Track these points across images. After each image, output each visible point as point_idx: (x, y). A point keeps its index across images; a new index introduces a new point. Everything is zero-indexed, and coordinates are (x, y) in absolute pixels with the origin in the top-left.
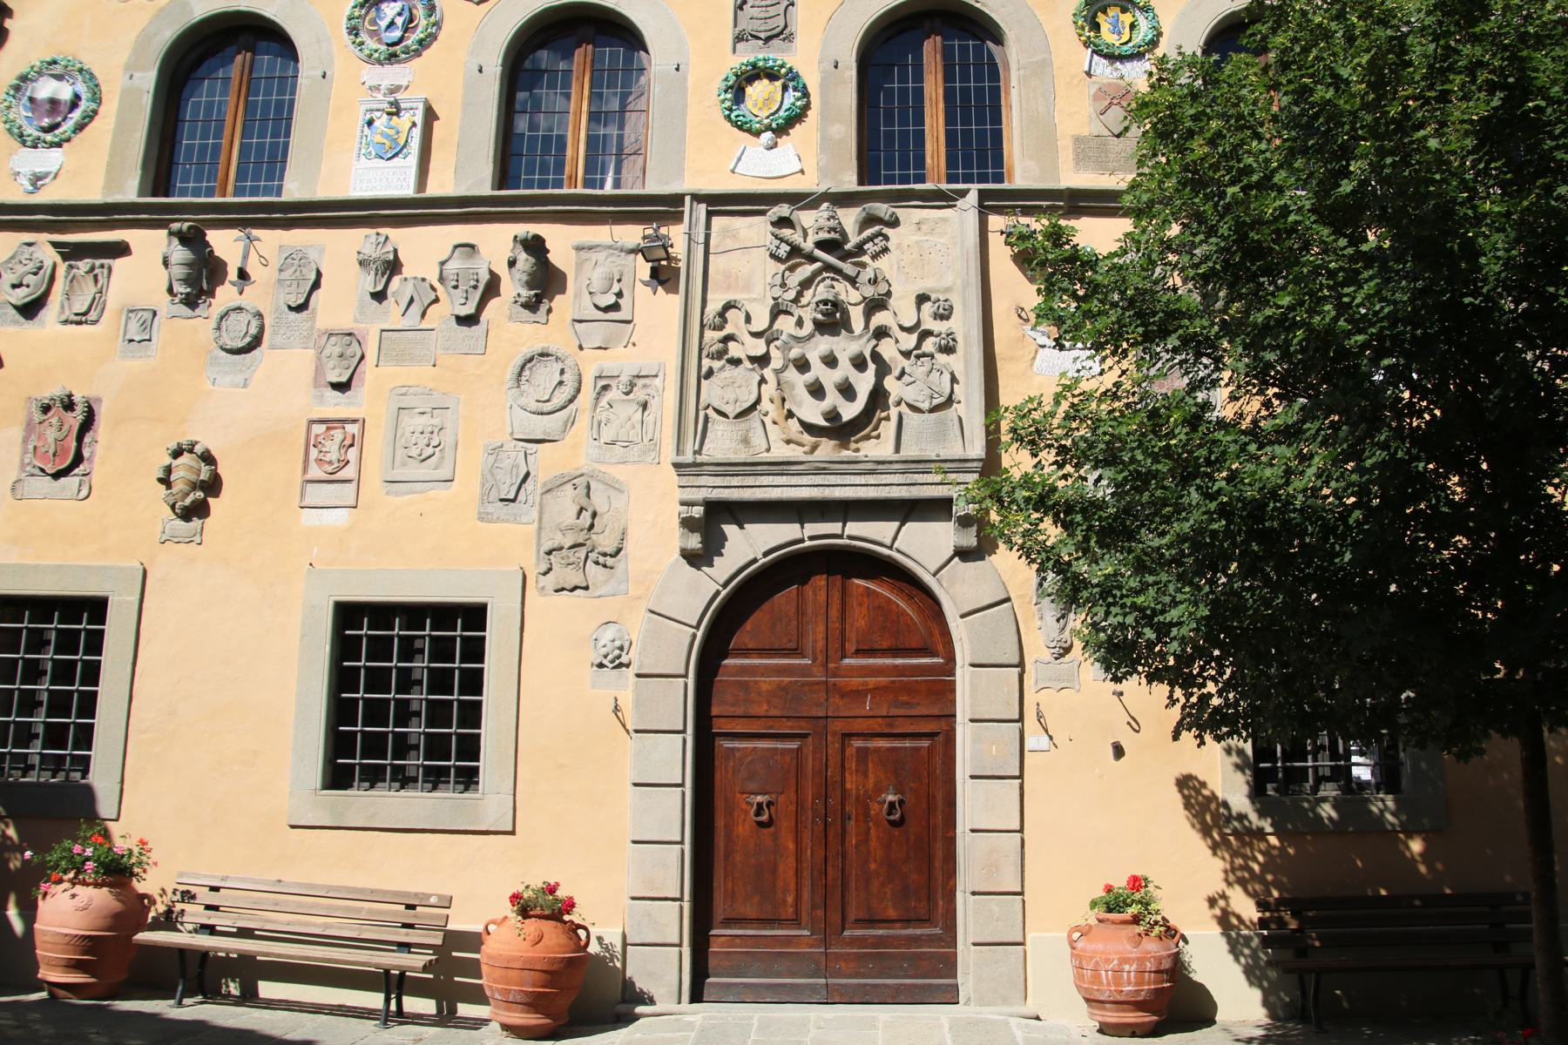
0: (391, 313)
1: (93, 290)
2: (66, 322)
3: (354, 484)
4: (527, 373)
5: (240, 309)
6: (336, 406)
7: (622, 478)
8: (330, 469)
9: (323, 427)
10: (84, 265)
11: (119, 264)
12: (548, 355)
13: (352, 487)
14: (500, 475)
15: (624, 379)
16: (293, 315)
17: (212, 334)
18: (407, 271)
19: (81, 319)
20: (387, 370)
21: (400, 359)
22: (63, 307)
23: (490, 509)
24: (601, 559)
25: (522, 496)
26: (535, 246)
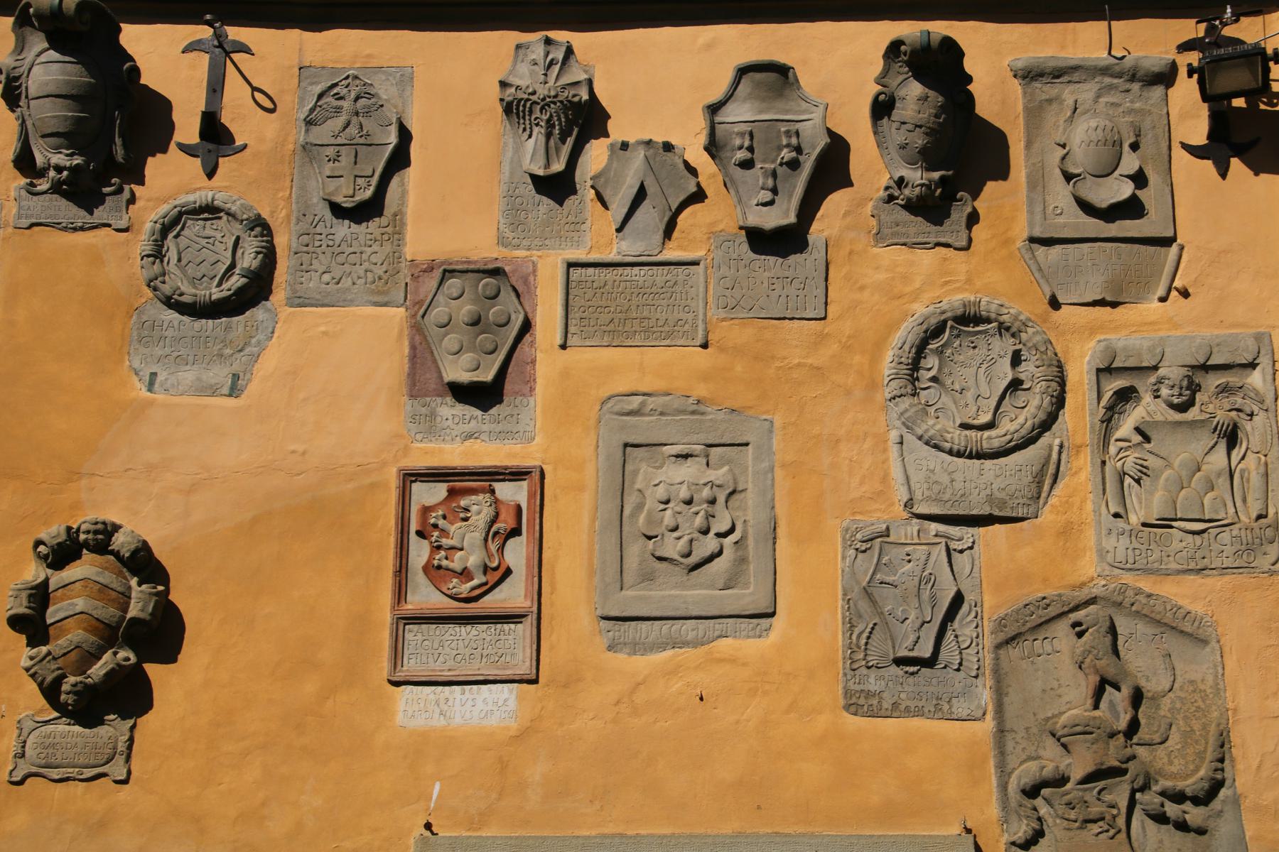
3: (529, 622)
4: (931, 361)
5: (210, 211)
6: (464, 441)
7: (1198, 608)
8: (465, 588)
9: (438, 492)
12: (977, 319)
13: (522, 631)
14: (889, 601)
15: (1172, 371)
16: (344, 229)
17: (138, 270)
20: (584, 357)
21: (621, 330)
23: (873, 682)
24: (1172, 809)
25: (949, 653)
26: (941, 67)
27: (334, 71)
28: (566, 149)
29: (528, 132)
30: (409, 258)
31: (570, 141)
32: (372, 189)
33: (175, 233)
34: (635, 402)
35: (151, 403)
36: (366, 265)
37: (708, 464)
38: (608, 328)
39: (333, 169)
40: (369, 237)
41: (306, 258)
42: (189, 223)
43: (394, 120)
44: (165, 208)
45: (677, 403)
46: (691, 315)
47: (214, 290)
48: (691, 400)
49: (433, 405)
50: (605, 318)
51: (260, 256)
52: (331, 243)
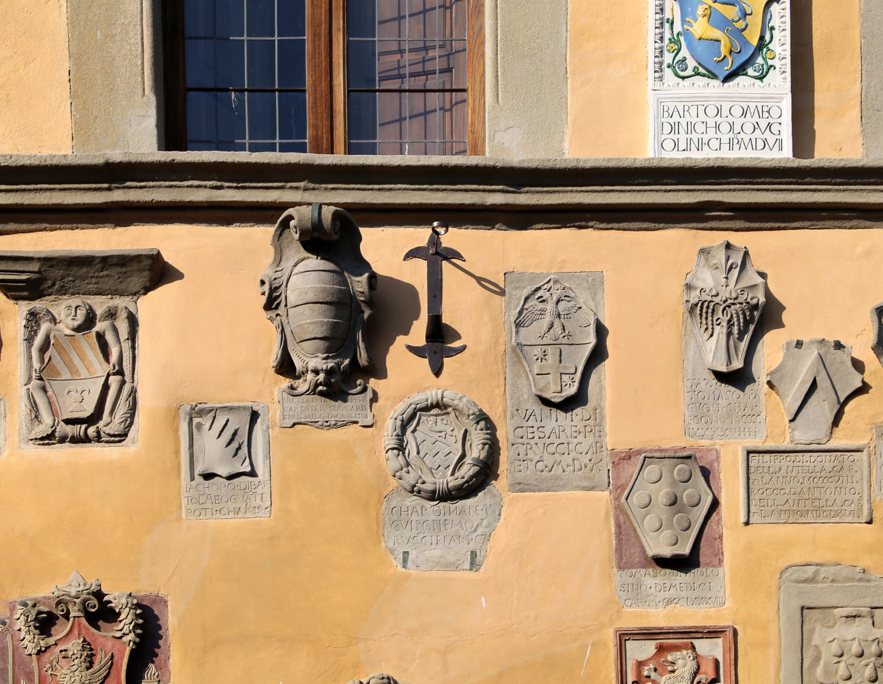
0: (769, 417)
1: (101, 368)
2: (49, 439)
5: (439, 406)
6: (668, 602)
9: (649, 648)
10: (65, 311)
11: (152, 307)
18: (795, 323)
19: (85, 429)
20: (766, 532)
21: (798, 512)
22: (34, 406)
27: (534, 277)
28: (743, 345)
29: (710, 330)
30: (610, 448)
31: (747, 338)
32: (576, 385)
33: (412, 428)
34: (810, 571)
35: (407, 578)
36: (573, 454)
37: (873, 624)
38: (784, 508)
39: (541, 368)
40: (574, 429)
41: (522, 449)
42: (423, 418)
43: (592, 321)
44: (400, 407)
45: (846, 572)
46: (857, 496)
47: (449, 478)
48: (858, 570)
49: (638, 575)
50: (781, 499)
51: (487, 447)
52: (542, 435)
